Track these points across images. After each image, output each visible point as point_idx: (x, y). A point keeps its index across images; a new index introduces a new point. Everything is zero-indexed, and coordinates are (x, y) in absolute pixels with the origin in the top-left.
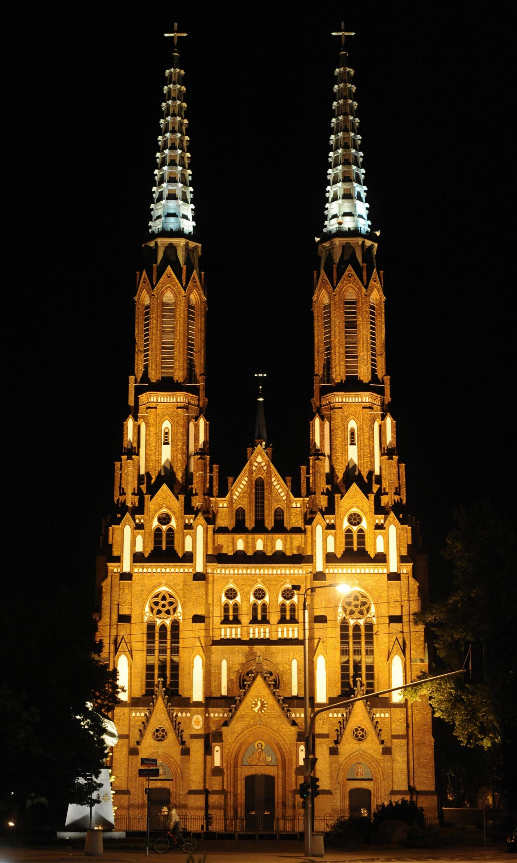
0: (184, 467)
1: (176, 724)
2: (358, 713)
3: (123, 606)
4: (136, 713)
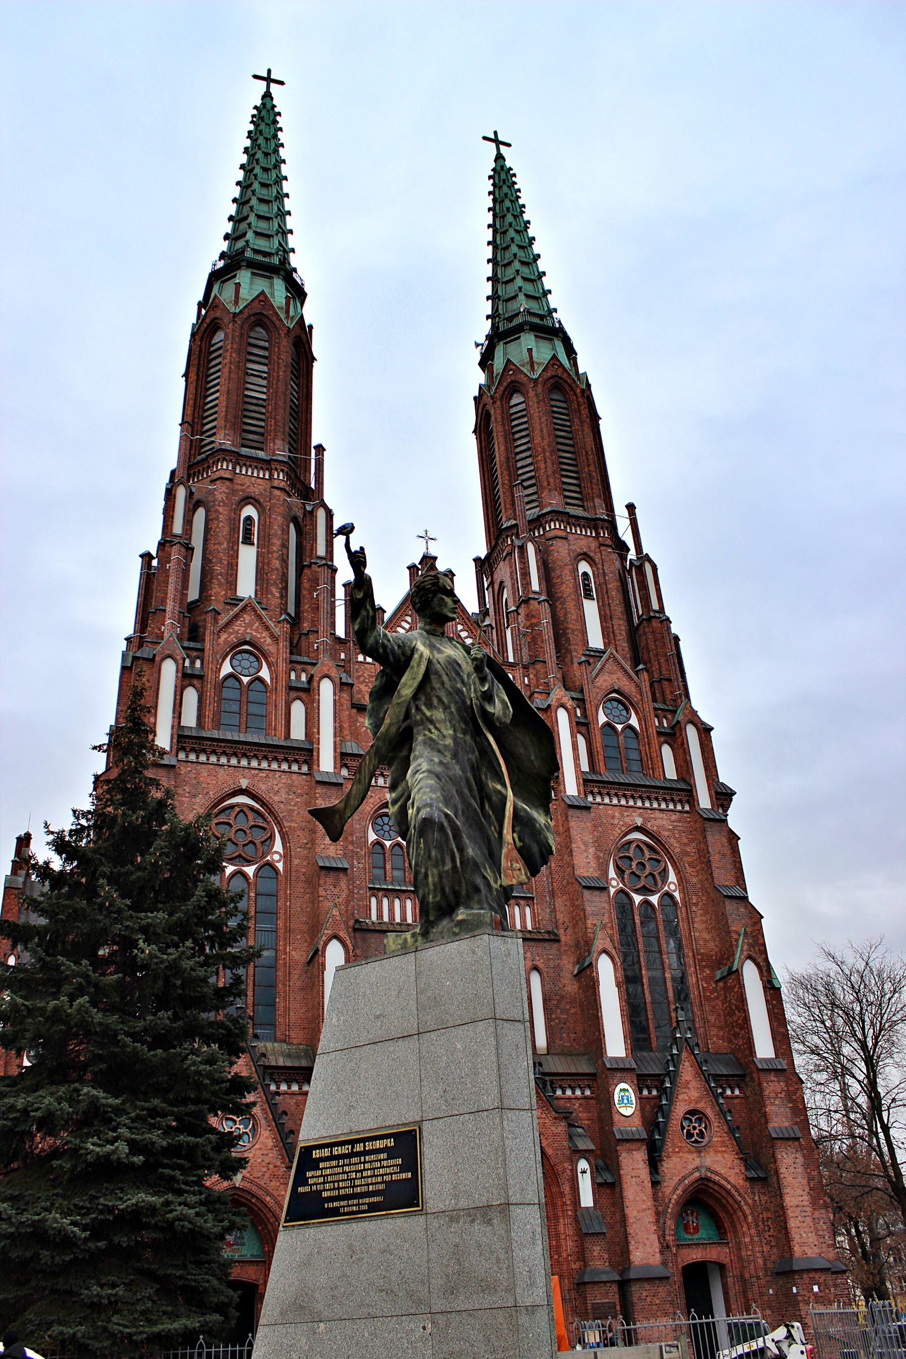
2: (688, 1082)
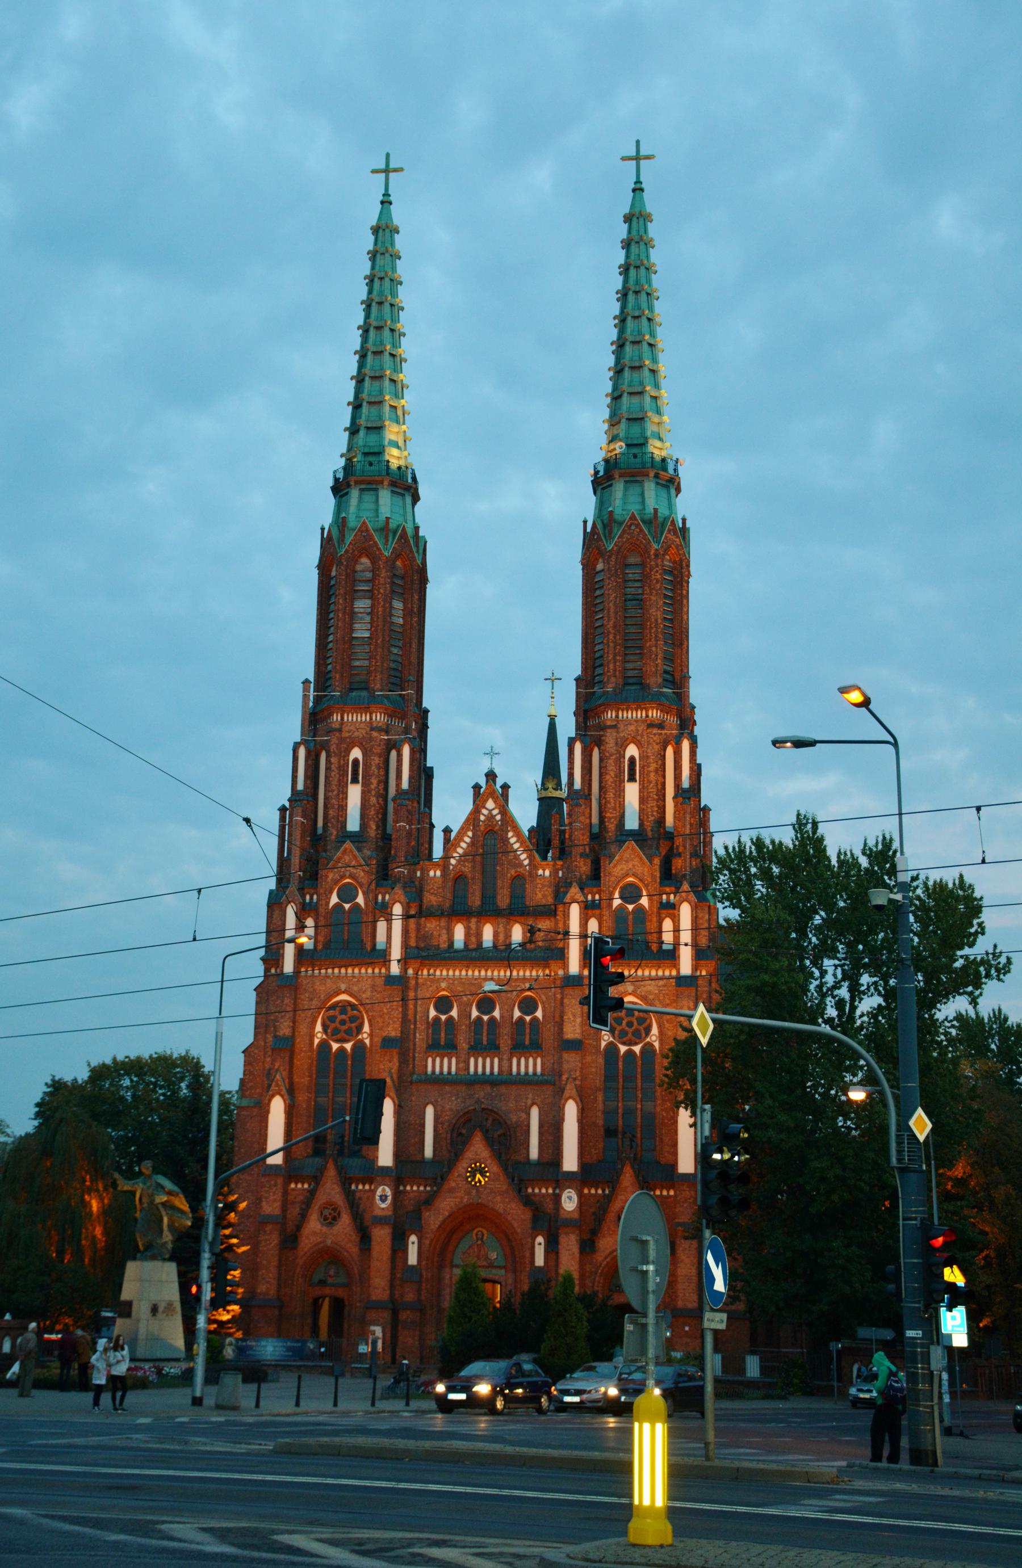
0: (380, 816)
1: (353, 1201)
2: (626, 1187)
3: (281, 1023)
4: (296, 1184)
